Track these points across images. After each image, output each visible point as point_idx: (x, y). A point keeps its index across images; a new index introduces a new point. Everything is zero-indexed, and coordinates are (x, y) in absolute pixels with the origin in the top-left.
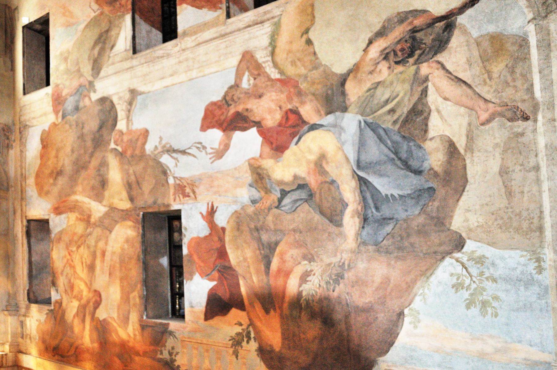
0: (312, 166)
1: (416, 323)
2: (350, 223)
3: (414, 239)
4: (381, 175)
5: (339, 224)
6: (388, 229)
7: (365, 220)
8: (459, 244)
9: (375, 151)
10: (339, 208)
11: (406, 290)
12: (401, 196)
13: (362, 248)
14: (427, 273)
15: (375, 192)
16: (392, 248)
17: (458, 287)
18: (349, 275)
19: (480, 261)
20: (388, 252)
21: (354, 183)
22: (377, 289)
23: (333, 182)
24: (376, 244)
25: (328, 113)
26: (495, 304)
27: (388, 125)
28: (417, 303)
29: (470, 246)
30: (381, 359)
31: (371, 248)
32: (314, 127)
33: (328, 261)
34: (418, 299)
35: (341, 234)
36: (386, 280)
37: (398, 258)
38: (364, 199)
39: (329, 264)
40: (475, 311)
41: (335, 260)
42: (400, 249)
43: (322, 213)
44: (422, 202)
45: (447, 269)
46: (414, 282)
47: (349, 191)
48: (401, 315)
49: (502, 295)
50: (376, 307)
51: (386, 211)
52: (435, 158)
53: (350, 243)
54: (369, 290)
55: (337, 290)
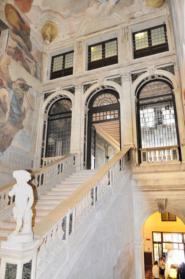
0: (3, 96)
1: (14, 141)
2: (7, 115)
3: (17, 124)
4: (15, 108)
5: (6, 114)
6: (14, 119)
7: (10, 115)
8: (23, 128)
9: (14, 102)
10: (6, 110)
11: (14, 133)
12: (17, 114)
13: (9, 121)
14: (18, 131)
15: (13, 110)
16: (13, 124)
17: (21, 136)
18: (5, 127)
19: (25, 132)
20: (13, 124)
21: (10, 106)
22: (10, 132)
23: (6, 103)
24: (11, 122)
25: (8, 87)
26: (25, 140)
27: (18, 98)
28: (15, 137)
29: (24, 129)
30: (8, 148)
31: (10, 122)
32: (5, 87)
33: (1, 121)
34: (16, 136)
35: (5, 116)
36: (11, 130)
37: (14, 126)
38: (11, 111)
39: (2, 122)
40: (22, 141)
41: (3, 122)
42: (15, 125)
43: (2, 109)
44: (20, 117)
45: (20, 132)
46: (16, 132)
47: (9, 107)
48: (12, 139)
49: (26, 139)
50: (9, 136)
51: (14, 115)
52: (23, 110)
53: (7, 119)
54: (8, 132)
55: (2, 129)
